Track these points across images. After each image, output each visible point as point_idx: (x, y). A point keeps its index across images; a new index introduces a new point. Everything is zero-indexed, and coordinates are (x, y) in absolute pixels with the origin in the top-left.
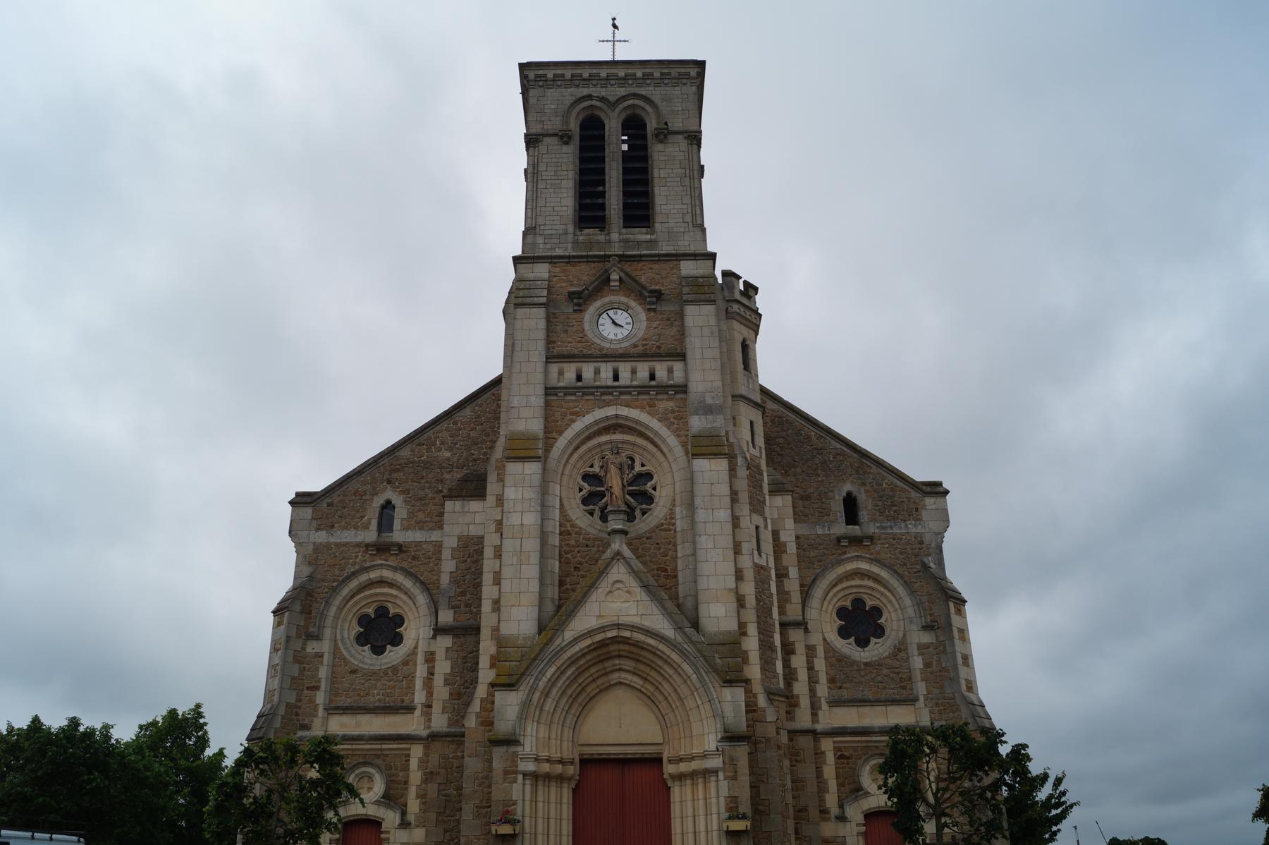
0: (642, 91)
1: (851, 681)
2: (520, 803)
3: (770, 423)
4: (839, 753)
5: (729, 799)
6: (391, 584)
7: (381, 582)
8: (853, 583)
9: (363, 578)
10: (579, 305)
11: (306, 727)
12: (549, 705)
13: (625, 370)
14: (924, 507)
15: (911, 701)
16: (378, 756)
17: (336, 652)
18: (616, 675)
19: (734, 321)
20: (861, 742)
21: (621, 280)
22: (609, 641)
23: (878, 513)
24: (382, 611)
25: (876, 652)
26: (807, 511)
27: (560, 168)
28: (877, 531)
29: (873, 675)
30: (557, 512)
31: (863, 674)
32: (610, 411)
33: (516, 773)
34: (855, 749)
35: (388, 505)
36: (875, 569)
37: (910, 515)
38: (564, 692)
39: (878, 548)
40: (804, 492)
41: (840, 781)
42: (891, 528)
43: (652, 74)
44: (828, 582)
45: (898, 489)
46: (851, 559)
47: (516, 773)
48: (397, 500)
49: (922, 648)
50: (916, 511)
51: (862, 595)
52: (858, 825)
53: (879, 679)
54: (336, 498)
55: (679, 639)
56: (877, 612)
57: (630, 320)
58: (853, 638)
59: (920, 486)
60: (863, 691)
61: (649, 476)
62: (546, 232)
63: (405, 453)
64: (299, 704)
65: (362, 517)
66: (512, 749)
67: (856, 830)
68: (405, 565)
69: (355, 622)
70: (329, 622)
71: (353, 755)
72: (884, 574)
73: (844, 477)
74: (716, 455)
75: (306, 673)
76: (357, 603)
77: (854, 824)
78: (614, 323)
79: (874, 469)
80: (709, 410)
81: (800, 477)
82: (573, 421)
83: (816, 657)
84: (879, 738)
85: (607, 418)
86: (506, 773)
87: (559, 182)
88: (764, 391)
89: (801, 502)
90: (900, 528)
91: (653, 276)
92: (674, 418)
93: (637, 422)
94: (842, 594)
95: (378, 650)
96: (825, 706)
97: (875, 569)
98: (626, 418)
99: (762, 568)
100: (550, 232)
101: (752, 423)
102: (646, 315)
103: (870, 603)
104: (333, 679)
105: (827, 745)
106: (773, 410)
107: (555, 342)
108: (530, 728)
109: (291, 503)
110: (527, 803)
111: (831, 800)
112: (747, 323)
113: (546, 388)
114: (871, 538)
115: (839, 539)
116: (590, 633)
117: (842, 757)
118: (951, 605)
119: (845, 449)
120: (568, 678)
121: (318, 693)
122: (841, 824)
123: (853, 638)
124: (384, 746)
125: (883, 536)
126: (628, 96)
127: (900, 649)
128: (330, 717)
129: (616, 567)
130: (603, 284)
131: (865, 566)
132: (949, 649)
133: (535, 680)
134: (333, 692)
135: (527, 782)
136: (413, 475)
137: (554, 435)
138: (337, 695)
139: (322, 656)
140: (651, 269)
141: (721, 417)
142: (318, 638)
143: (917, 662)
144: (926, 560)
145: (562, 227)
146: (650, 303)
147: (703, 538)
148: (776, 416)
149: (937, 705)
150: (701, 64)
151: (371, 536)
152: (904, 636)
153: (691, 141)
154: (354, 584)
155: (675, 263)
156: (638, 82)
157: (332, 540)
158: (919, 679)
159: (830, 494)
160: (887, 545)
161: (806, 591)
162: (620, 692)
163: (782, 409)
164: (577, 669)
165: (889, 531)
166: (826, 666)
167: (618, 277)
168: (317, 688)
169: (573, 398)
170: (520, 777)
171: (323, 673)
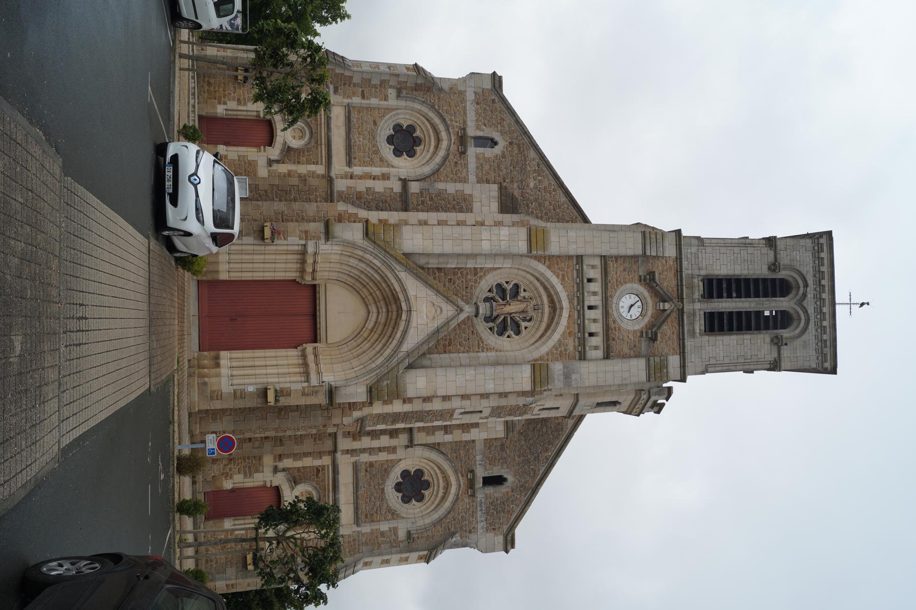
0: (812, 326)
1: (371, 478)
2: (285, 242)
3: (557, 422)
4: (321, 469)
5: (289, 390)
6: (437, 147)
7: (438, 141)
8: (441, 481)
9: (441, 127)
10: (645, 280)
11: (336, 91)
12: (353, 262)
13: (597, 314)
14: (496, 534)
15: (357, 522)
16: (316, 143)
17: (388, 110)
18: (375, 310)
19: (634, 395)
20: (328, 485)
21: (664, 310)
22: (399, 304)
23: (491, 500)
24: (417, 142)
25: (391, 497)
26: (493, 448)
27: (749, 263)
28: (478, 499)
29: (375, 495)
30: (491, 266)
31: (376, 487)
32: (565, 304)
33: (306, 239)
34: (323, 481)
35: (494, 143)
36: (451, 498)
37: (490, 524)
38: (362, 272)
39: (466, 500)
40: (507, 447)
41: (301, 469)
42: (481, 510)
43: (825, 333)
44: (441, 463)
45: (509, 516)
46: (458, 480)
47: (306, 239)
48: (497, 150)
49: (395, 530)
50: (493, 529)
51: (431, 490)
52: (271, 481)
53: (373, 499)
54: (498, 105)
55: (401, 355)
56: (420, 498)
57: (634, 317)
58: (402, 481)
59: (512, 532)
60: (364, 487)
61: (518, 332)
62: (700, 254)
63: (532, 154)
64: (352, 85)
65: (485, 125)
66: (323, 236)
67: (268, 480)
68: (451, 157)
69: (410, 122)
70: (410, 104)
71: (317, 125)
72: (448, 504)
73: (518, 476)
74: (534, 382)
75: (373, 90)
76: (424, 123)
77: (272, 478)
78: (632, 306)
79: (524, 499)
80: (567, 376)
81: (517, 444)
82: (558, 277)
83: (388, 454)
84: (331, 498)
85: (560, 302)
86: (306, 232)
87: (739, 262)
88: (581, 418)
89: (499, 444)
90: (481, 517)
91: (668, 335)
92: (561, 351)
93: (558, 323)
94: (433, 473)
95: (390, 140)
96: (354, 459)
97: (451, 498)
98: (560, 315)
99: (452, 415)
100: (700, 257)
101: (558, 408)
102: (638, 330)
103: (426, 493)
104: (370, 109)
105: (326, 461)
106: (567, 425)
107: (616, 262)
108: (337, 249)
109: (494, 73)
110: (285, 248)
111: (288, 463)
112: (632, 405)
113: (582, 256)
114: (473, 495)
115: (472, 471)
116: (404, 290)
117: (318, 471)
118: (425, 553)
119: (539, 477)
120: (372, 275)
121: (360, 98)
122: (271, 469)
123: (402, 481)
124: (323, 146)
125: (475, 504)
126: (808, 315)
127: (394, 514)
128: (343, 108)
129: (452, 309)
130: (662, 297)
131: (453, 490)
132: (394, 550)
133: (372, 252)
134: (360, 109)
135: (300, 247)
136: (516, 160)
137: (547, 263)
138: (359, 112)
139: (385, 100)
140: (673, 333)
141: (562, 386)
142: (398, 96)
143: (384, 527)
144: (458, 535)
145: (704, 266)
146: (647, 333)
147: (473, 372)
148: (562, 426)
149: (354, 540)
150: (834, 371)
151: (472, 132)
152: (403, 518)
153: (773, 364)
154: (437, 121)
155: (678, 351)
156: (819, 323)
157: (468, 104)
158: (373, 528)
159: (506, 465)
160: (468, 507)
161: (435, 447)
162: (362, 313)
163: (568, 430)
164: (379, 281)
165: (479, 508)
166: (381, 461)
167: (666, 308)
168: (363, 97)
169: (575, 276)
170: (303, 242)
171: (374, 101)
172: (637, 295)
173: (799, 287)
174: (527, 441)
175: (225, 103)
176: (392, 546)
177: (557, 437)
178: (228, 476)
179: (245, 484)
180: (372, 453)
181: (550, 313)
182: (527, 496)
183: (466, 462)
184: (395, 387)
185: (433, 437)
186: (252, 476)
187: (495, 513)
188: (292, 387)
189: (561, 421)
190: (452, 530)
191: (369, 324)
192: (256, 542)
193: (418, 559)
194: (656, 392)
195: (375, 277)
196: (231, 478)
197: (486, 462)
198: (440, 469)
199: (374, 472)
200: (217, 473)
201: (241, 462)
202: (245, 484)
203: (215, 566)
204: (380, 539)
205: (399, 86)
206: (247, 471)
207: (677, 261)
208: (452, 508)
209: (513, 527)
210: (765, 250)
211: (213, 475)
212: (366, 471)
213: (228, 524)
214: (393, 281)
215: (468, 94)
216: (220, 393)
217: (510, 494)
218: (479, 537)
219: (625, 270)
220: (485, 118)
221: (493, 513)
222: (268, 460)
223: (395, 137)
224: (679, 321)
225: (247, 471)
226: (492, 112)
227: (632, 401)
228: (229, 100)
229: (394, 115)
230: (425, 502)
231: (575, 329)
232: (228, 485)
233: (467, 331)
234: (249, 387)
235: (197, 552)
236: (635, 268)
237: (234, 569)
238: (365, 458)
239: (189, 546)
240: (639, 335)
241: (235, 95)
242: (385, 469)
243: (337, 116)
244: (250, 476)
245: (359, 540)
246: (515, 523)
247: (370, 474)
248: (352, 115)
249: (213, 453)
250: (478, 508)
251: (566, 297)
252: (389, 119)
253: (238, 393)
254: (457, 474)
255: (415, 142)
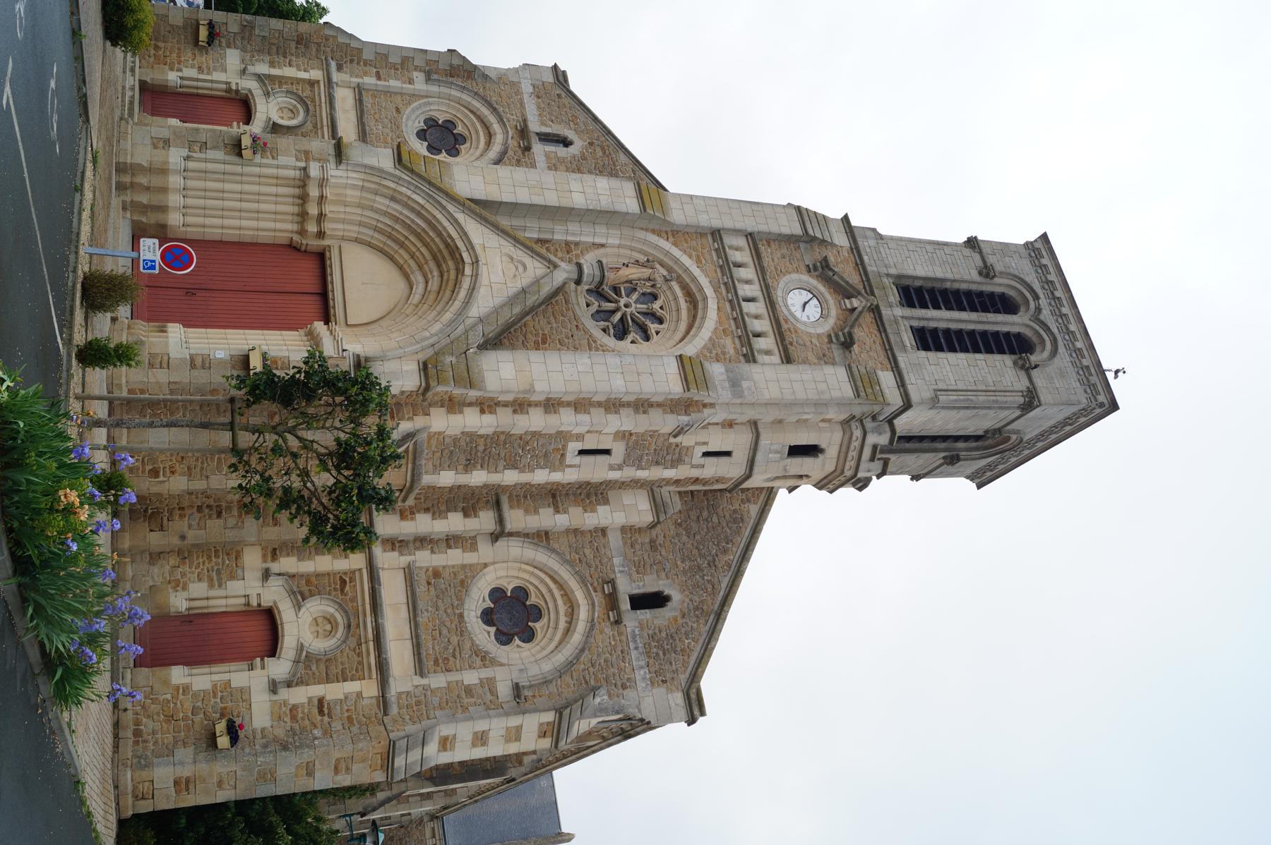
0: (1061, 349)
1: (438, 597)
2: (275, 162)
3: (732, 508)
4: (348, 580)
5: (286, 361)
6: (489, 143)
7: (490, 136)
8: (560, 602)
9: (492, 119)
10: (815, 269)
11: (340, 68)
12: (382, 203)
13: (758, 307)
14: (670, 691)
15: (420, 670)
16: (315, 126)
17: (415, 96)
18: (420, 279)
19: (842, 433)
20: (364, 605)
21: (854, 309)
22: (458, 256)
23: (651, 632)
24: (460, 139)
25: (478, 631)
26: (638, 547)
27: (952, 266)
28: (629, 630)
29: (448, 624)
30: (589, 239)
31: (449, 611)
32: (709, 291)
33: (307, 160)
34: (354, 599)
35: (566, 143)
36: (581, 627)
37: (656, 672)
38: (397, 220)
39: (608, 630)
40: (660, 545)
41: (313, 579)
42: (636, 648)
43: (1083, 357)
44: (556, 569)
45: (686, 658)
46: (588, 596)
47: (307, 160)
48: (572, 150)
49: (490, 684)
50: (663, 681)
51: (546, 617)
52: (259, 595)
53: (445, 631)
54: (566, 100)
55: (469, 322)
56: (529, 636)
57: (812, 319)
58: (492, 606)
59: (694, 685)
60: (427, 611)
61: (647, 338)
62: (882, 249)
63: (622, 158)
64: (362, 63)
65: (552, 121)
66: (332, 160)
67: (253, 593)
68: (510, 153)
69: (448, 117)
70: (444, 90)
71: (315, 106)
72: (577, 637)
73: (687, 592)
74: (685, 379)
75: (393, 71)
76: (466, 116)
77: (260, 591)
78: (805, 304)
79: (705, 629)
80: (735, 384)
81: (676, 541)
82: (690, 257)
83: (464, 551)
84: (369, 625)
85: (701, 289)
86: (307, 153)
87: (937, 262)
88: (769, 496)
89: (647, 540)
90: (638, 659)
91: (868, 343)
92: (717, 354)
93: (704, 318)
94: (544, 590)
95: (421, 135)
96: (404, 560)
97: (581, 627)
98: (705, 307)
99: (563, 455)
100: (883, 253)
101: (728, 454)
102: (823, 334)
103: (537, 626)
104: (388, 93)
105: (356, 560)
106: (748, 512)
107: (769, 246)
108: (355, 178)
109: (555, 66)
110: (274, 171)
111: (288, 564)
112: (842, 455)
113: (719, 231)
114: (618, 622)
115: (612, 582)
116: (464, 235)
117: (343, 582)
118: (549, 717)
119: (722, 593)
120: (413, 221)
121: (375, 79)
122: (259, 574)
123: (492, 606)
124: (325, 129)
125: (624, 638)
126: (1052, 334)
127: (486, 659)
128: (352, 90)
129: (540, 265)
130: (844, 291)
131: (583, 613)
132: (492, 712)
133: (410, 183)
134: (376, 93)
135: (298, 172)
136: (602, 164)
137: (671, 239)
138: (374, 96)
139: (410, 83)
140: (874, 342)
141: (730, 396)
142: (428, 79)
143: (471, 678)
144: (603, 691)
145: (892, 264)
146: (837, 336)
147: (587, 361)
148: (742, 514)
149: (418, 703)
150: (1114, 406)
151: (535, 126)
152: (502, 665)
153: (1027, 396)
154: (485, 111)
155: (889, 366)
156: (1070, 345)
157: (526, 97)
158: (450, 679)
159: (664, 574)
160: (613, 643)
161: (542, 537)
162: (401, 285)
163: (752, 521)
164: (424, 230)
165: (632, 645)
166: (453, 566)
167: (856, 306)
168: (379, 78)
169: (715, 258)
170: (303, 164)
171: (394, 84)
172: (809, 291)
173: (1028, 301)
174: (692, 536)
175: (180, 70)
176: (488, 708)
177: (738, 532)
178: (179, 585)
179: (212, 603)
180: (436, 549)
181: (689, 310)
182: (709, 625)
183: (597, 566)
184: (466, 372)
185: (536, 517)
186: (224, 586)
187: (661, 653)
188: (291, 355)
189: (738, 507)
190: (593, 683)
191: (413, 299)
192: (232, 429)
193: (539, 737)
194: (872, 428)
195: (418, 224)
196: (184, 589)
197: (630, 569)
198: (555, 581)
199: (443, 586)
200: (159, 580)
201: (204, 563)
202: (212, 603)
203: (152, 748)
204: (466, 701)
205: (427, 68)
206: (215, 578)
207: (853, 253)
208: (586, 642)
209: (695, 677)
210: (967, 252)
211: (151, 584)
212: (429, 583)
213: (178, 674)
214: (446, 224)
215: (523, 85)
216: (166, 358)
217: (680, 621)
218: (641, 695)
219: (783, 257)
220: (550, 114)
221: (657, 654)
222: (252, 559)
223: (428, 133)
224: (878, 326)
225: (215, 578)
226: (559, 107)
227: (841, 445)
228: (187, 67)
229: (425, 104)
230: (537, 642)
231: (730, 326)
232: (179, 603)
233: (569, 326)
234: (217, 352)
235: (110, 438)
236: (798, 256)
237: (191, 750)
238: (424, 559)
239: (98, 423)
240: (826, 340)
241: (195, 62)
242: (463, 579)
243: (344, 99)
244: (220, 586)
245: (426, 702)
246: (697, 669)
247: (436, 589)
248: (365, 99)
249: (153, 267)
250: (631, 644)
251: (708, 284)
252: (417, 108)
253: (199, 361)
254: (586, 585)
255: (456, 140)
